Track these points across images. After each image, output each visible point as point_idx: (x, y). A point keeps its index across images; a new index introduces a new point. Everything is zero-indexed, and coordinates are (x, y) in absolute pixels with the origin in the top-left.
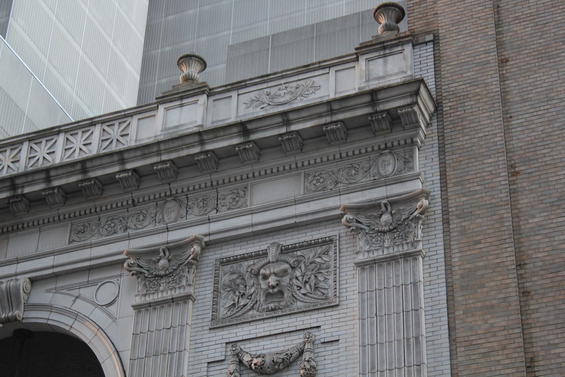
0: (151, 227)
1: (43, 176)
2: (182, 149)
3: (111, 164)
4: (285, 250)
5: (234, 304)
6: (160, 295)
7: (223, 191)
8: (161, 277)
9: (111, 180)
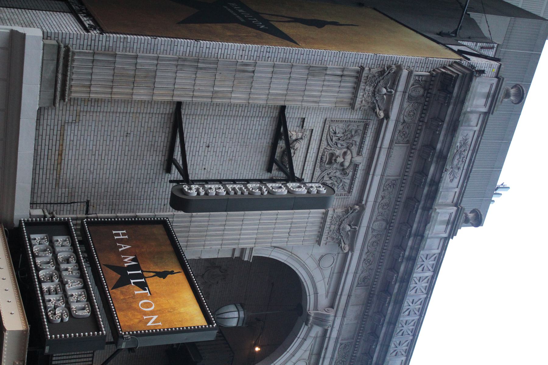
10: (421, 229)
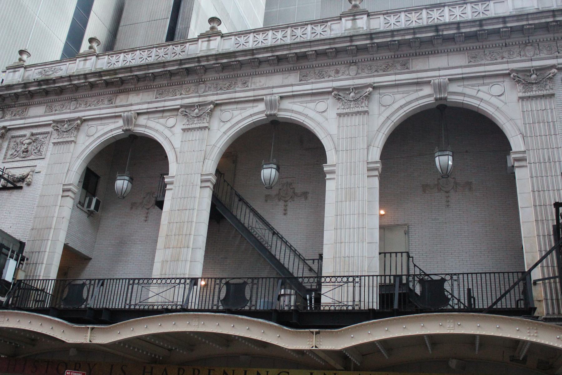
0: (518, 58)
1: (456, 26)
2: (542, 19)
9: (497, 32)
10: (66, 79)
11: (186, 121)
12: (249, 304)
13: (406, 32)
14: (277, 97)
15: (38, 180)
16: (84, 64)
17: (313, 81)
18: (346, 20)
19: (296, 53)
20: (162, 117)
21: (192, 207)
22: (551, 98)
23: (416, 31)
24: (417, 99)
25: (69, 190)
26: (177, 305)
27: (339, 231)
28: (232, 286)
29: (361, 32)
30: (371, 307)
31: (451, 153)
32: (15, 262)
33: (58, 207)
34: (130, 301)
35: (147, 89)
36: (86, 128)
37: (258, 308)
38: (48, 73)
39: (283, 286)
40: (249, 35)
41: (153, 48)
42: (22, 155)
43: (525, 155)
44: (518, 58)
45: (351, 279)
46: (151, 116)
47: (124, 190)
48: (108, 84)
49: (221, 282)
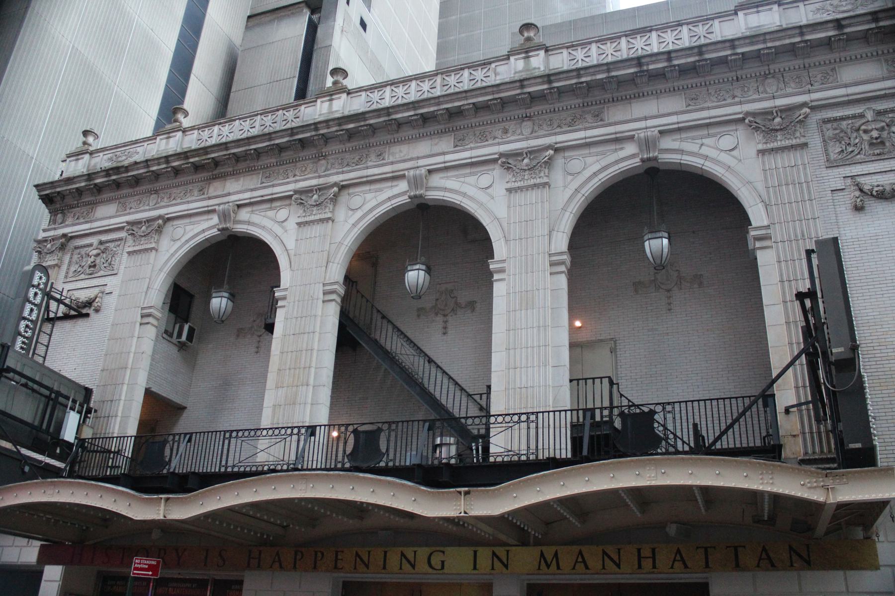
0: (756, 96)
3: (724, 49)
4: (879, 113)
5: (842, 151)
6: (779, 143)
7: (813, 72)
8: (777, 130)
9: (723, 61)
11: (301, 211)
12: (384, 459)
13: (598, 69)
14: (423, 171)
15: (110, 304)
16: (167, 143)
17: (472, 145)
18: (516, 60)
19: (447, 109)
20: (271, 209)
21: (311, 329)
22: (802, 149)
23: (611, 67)
24: (617, 162)
25: (149, 315)
26: (288, 465)
27: (512, 352)
28: (361, 435)
29: (537, 74)
30: (552, 455)
31: (666, 235)
32: (78, 416)
33: (135, 340)
34: (227, 461)
35: (250, 171)
36: (172, 229)
37: (397, 464)
38: (120, 159)
39: (431, 432)
40: (384, 89)
41: (257, 115)
42: (88, 271)
43: (769, 231)
44: (756, 96)
45: (524, 418)
46: (255, 208)
47: (222, 310)
48: (197, 168)
49: (346, 429)
